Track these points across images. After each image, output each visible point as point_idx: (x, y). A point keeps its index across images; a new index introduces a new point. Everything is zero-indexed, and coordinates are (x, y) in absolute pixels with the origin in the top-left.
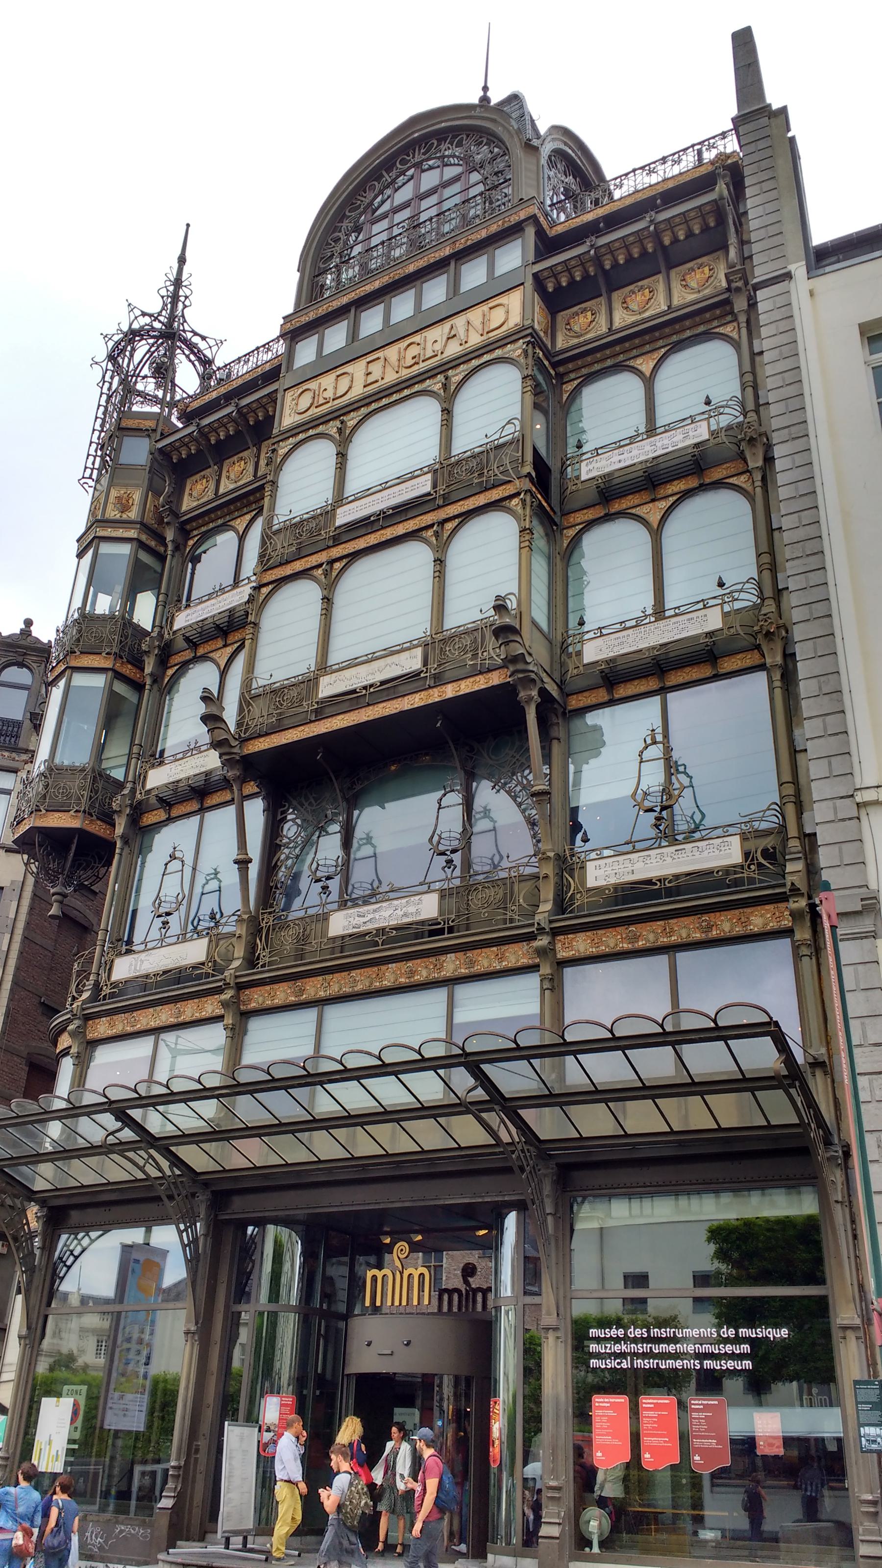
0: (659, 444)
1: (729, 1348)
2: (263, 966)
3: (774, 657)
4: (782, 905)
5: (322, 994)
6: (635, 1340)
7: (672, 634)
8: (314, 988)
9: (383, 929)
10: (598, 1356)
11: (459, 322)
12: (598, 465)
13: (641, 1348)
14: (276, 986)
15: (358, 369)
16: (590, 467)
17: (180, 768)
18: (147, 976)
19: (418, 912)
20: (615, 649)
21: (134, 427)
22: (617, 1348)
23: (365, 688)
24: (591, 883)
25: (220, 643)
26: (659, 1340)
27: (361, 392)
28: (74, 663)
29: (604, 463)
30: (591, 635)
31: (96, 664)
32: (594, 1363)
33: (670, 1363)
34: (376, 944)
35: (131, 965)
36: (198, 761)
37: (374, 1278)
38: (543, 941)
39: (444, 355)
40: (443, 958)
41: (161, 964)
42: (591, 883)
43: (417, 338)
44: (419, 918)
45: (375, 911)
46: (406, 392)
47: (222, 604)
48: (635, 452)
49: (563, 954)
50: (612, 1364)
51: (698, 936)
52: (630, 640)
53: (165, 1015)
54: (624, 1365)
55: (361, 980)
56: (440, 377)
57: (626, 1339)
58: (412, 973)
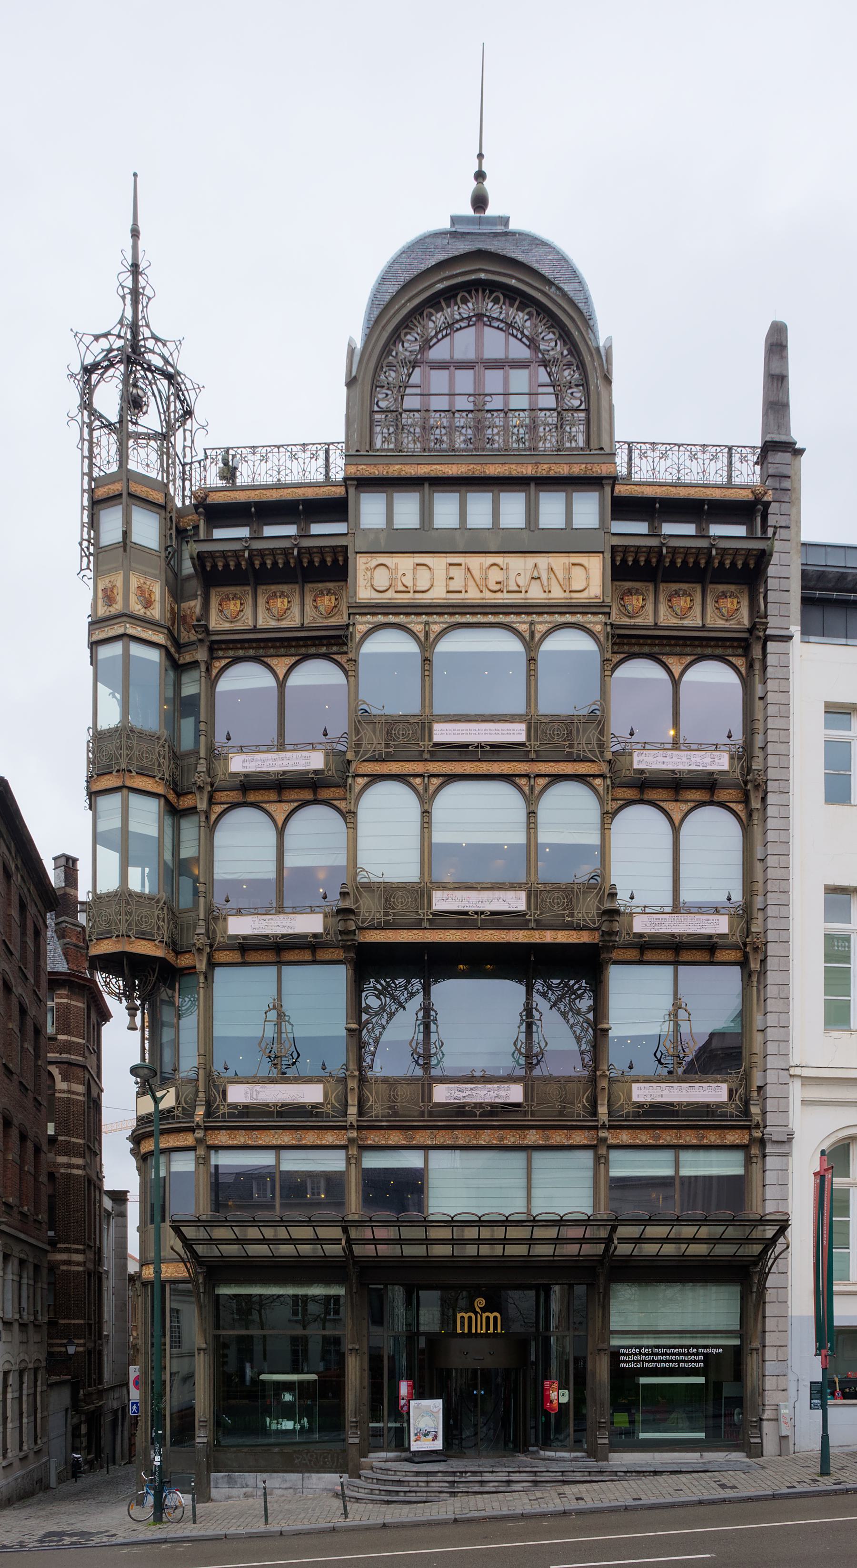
0: (693, 760)
1: (693, 1358)
3: (756, 964)
4: (746, 1131)
5: (429, 1142)
6: (645, 1354)
7: (695, 928)
12: (646, 759)
13: (647, 1358)
14: (390, 1132)
16: (641, 758)
17: (264, 923)
18: (267, 1105)
19: (507, 1096)
20: (656, 927)
21: (143, 495)
22: (635, 1358)
24: (635, 1098)
26: (657, 1354)
29: (650, 759)
30: (639, 910)
31: (149, 788)
32: (622, 1365)
33: (663, 1365)
35: (246, 1093)
36: (284, 921)
38: (603, 1134)
40: (527, 1132)
41: (278, 1097)
44: (508, 1101)
45: (472, 1089)
48: (675, 759)
49: (611, 1141)
50: (631, 1365)
51: (695, 1142)
52: (667, 923)
53: (286, 1138)
54: (639, 1366)
57: (640, 1354)
58: (503, 1138)
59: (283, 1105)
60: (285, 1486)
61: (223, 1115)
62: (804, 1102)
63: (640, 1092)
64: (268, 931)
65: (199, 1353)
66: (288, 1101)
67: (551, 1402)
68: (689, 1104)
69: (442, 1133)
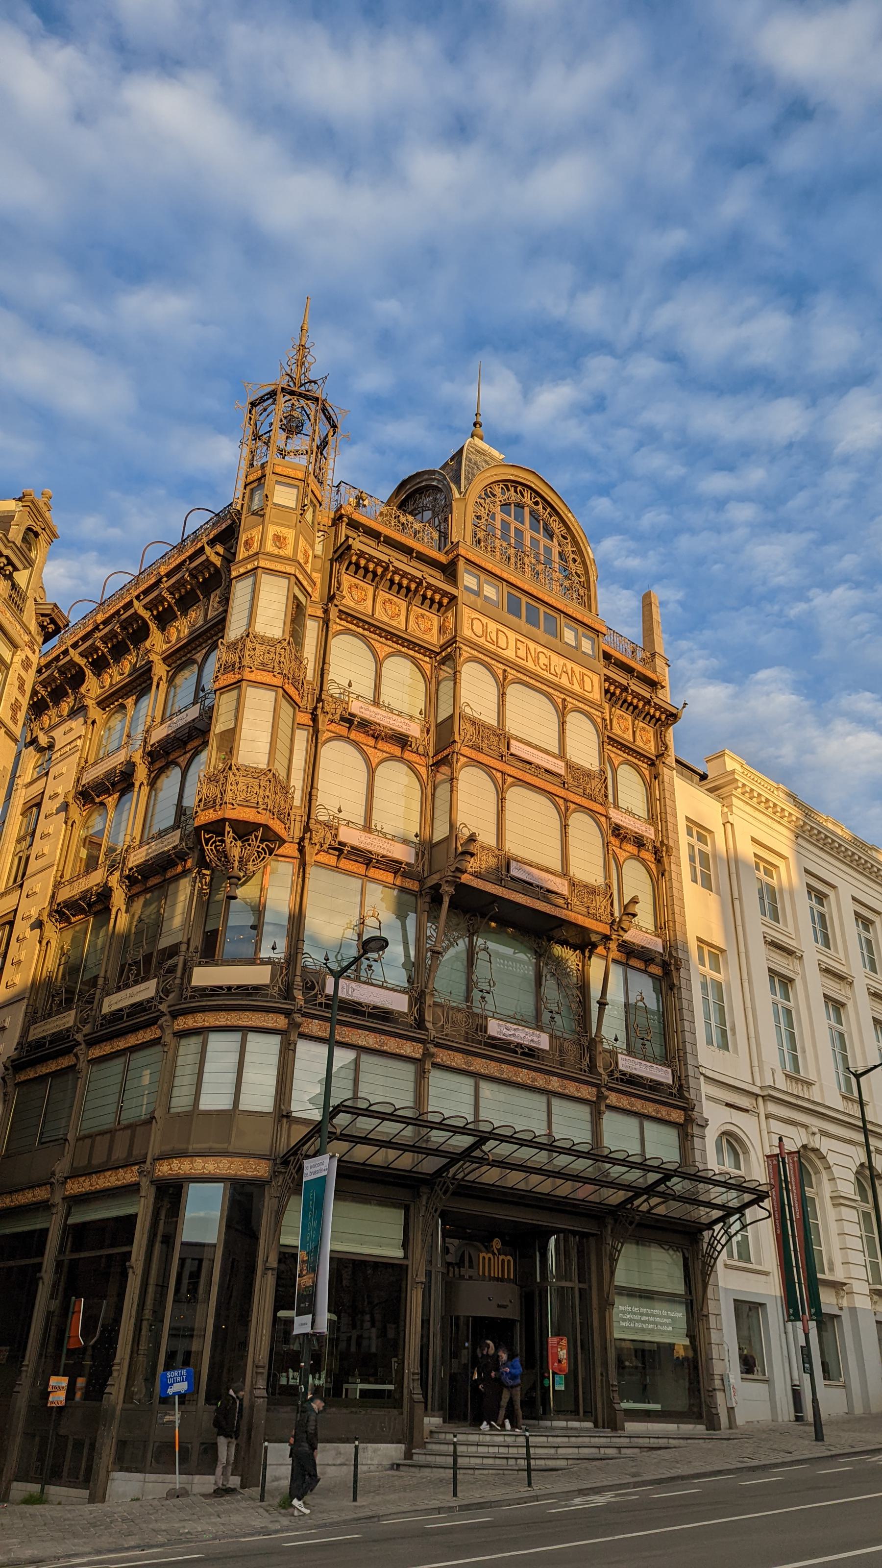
2: (447, 1035)
8: (479, 1065)
9: (521, 1044)
10: (624, 1320)
11: (570, 665)
13: (637, 1317)
14: (456, 1054)
15: (512, 636)
18: (360, 1004)
19: (539, 1043)
23: (538, 886)
24: (621, 1067)
25: (371, 742)
26: (642, 1314)
27: (514, 657)
28: (286, 687)
34: (516, 1052)
36: (385, 845)
37: (484, 1258)
39: (561, 681)
42: (621, 1067)
43: (545, 651)
45: (515, 1030)
46: (538, 684)
47: (392, 722)
55: (506, 1072)
56: (563, 696)
58: (534, 1080)
59: (375, 1007)
60: (338, 1462)
61: (320, 1004)
62: (709, 1098)
63: (624, 1062)
64: (371, 848)
65: (264, 1274)
66: (379, 1004)
67: (560, 1361)
68: (652, 1080)
69: (493, 1064)
